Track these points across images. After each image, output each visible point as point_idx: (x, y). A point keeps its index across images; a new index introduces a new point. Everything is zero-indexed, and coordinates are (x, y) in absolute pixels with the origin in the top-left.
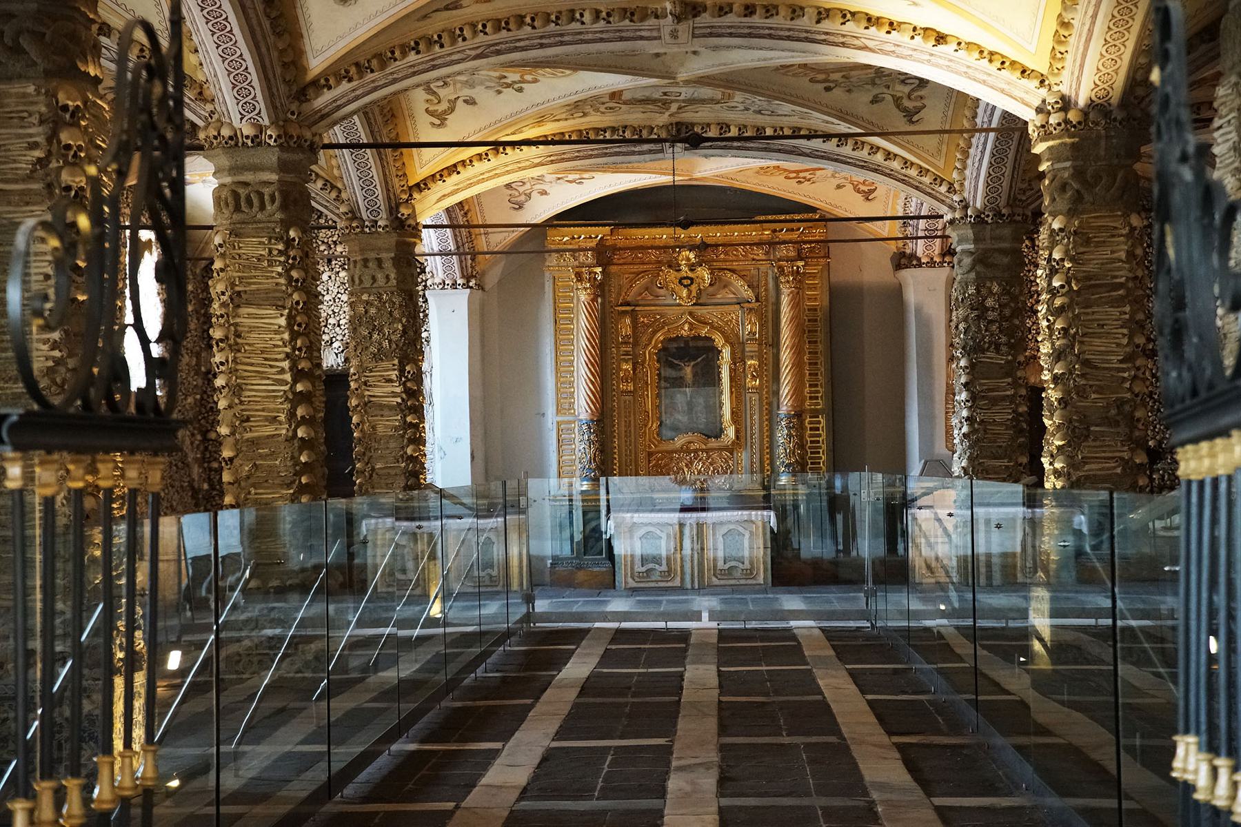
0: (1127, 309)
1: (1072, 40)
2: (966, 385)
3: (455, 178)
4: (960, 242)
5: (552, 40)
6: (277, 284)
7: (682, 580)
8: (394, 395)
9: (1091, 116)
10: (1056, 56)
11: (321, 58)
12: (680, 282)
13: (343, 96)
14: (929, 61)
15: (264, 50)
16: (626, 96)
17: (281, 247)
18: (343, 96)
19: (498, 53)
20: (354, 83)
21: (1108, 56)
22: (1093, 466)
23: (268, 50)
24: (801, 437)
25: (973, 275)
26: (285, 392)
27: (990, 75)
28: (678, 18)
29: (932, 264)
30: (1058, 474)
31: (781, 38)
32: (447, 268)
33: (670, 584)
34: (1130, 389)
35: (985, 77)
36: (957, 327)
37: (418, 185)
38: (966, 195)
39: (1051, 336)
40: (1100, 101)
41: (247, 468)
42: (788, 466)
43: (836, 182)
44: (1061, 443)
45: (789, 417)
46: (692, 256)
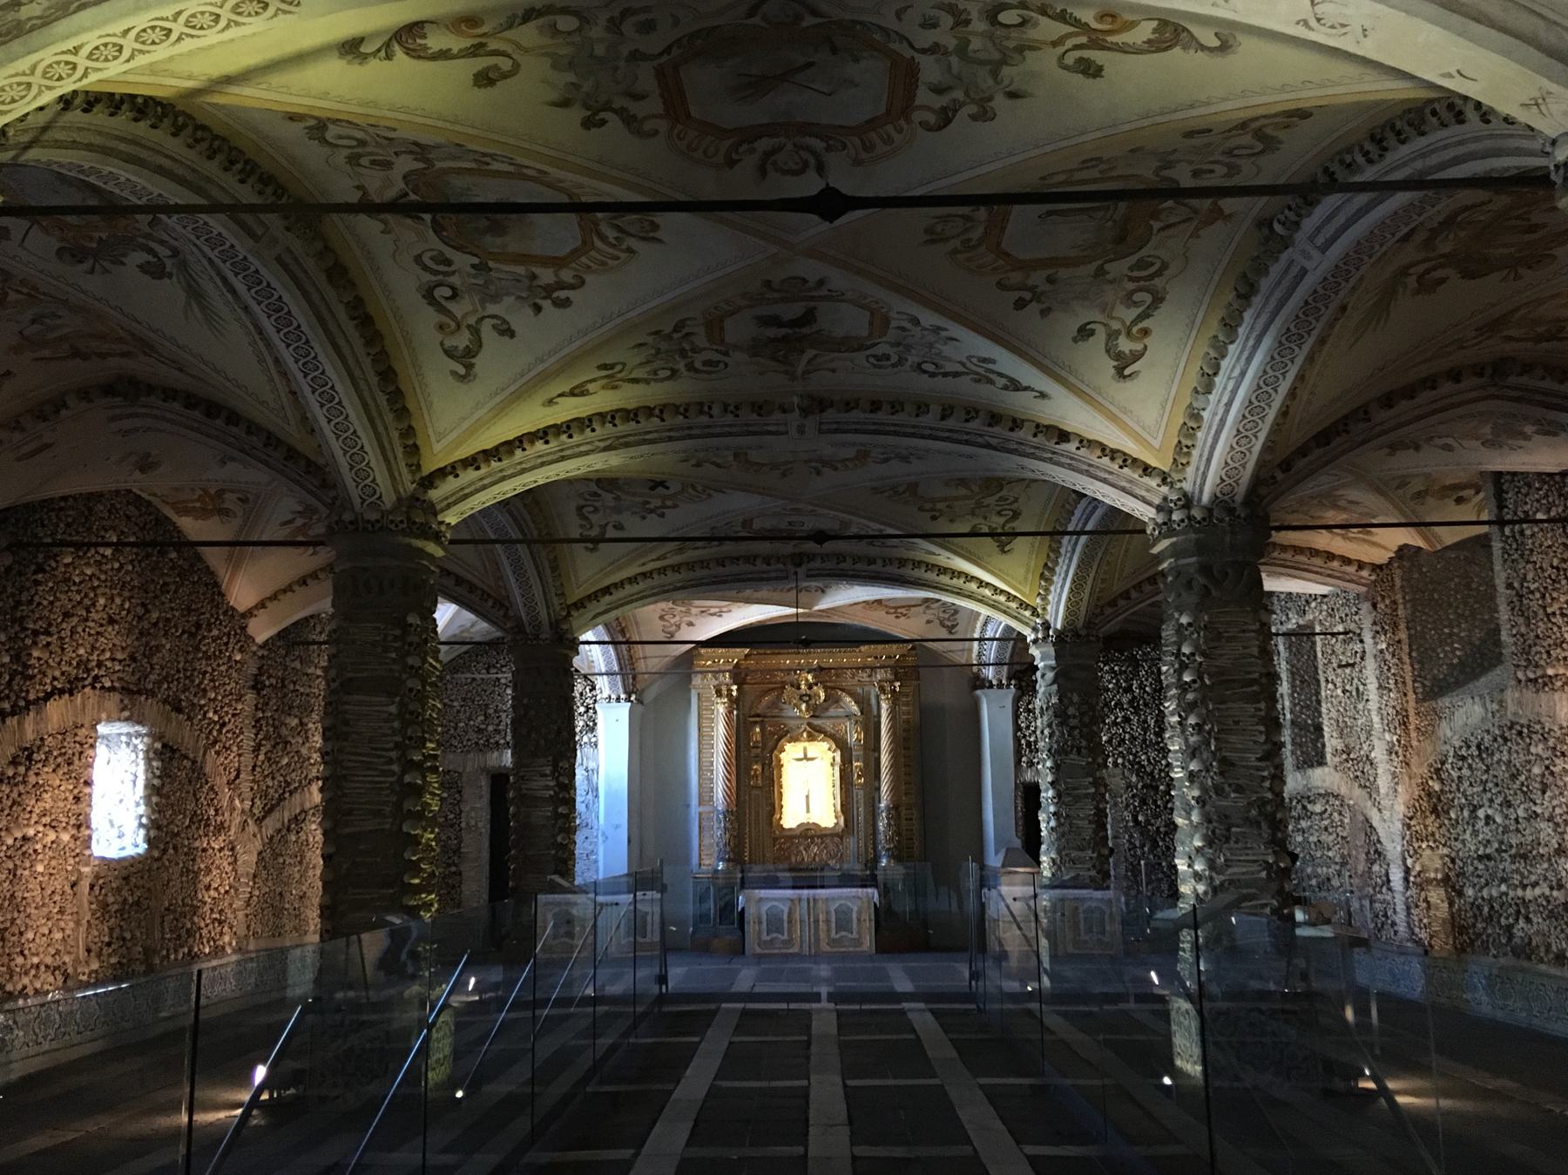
0: (1262, 705)
1: (1199, 434)
2: (1052, 784)
3: (608, 598)
4: (1042, 659)
5: (680, 433)
6: (391, 670)
7: (801, 947)
8: (548, 788)
9: (1216, 513)
10: (1183, 450)
11: (444, 442)
12: (801, 698)
13: (470, 485)
14: (1051, 459)
15: (381, 429)
16: (757, 525)
17: (398, 632)
18: (470, 485)
19: (627, 445)
20: (483, 471)
21: (1238, 449)
22: (1235, 870)
23: (386, 429)
24: (898, 826)
25: (1055, 687)
26: (391, 783)
27: (1111, 473)
28: (805, 412)
29: (1000, 686)
30: (1197, 876)
31: (906, 435)
32: (613, 686)
33: (791, 951)
34: (1270, 789)
35: (1107, 476)
36: (1042, 732)
37: (575, 604)
38: (1048, 618)
39: (1183, 732)
40: (1226, 498)
41: (345, 866)
42: (888, 850)
43: (926, 617)
44: (1200, 844)
45: (887, 807)
46: (810, 677)
